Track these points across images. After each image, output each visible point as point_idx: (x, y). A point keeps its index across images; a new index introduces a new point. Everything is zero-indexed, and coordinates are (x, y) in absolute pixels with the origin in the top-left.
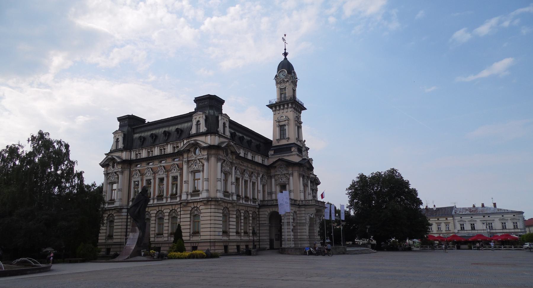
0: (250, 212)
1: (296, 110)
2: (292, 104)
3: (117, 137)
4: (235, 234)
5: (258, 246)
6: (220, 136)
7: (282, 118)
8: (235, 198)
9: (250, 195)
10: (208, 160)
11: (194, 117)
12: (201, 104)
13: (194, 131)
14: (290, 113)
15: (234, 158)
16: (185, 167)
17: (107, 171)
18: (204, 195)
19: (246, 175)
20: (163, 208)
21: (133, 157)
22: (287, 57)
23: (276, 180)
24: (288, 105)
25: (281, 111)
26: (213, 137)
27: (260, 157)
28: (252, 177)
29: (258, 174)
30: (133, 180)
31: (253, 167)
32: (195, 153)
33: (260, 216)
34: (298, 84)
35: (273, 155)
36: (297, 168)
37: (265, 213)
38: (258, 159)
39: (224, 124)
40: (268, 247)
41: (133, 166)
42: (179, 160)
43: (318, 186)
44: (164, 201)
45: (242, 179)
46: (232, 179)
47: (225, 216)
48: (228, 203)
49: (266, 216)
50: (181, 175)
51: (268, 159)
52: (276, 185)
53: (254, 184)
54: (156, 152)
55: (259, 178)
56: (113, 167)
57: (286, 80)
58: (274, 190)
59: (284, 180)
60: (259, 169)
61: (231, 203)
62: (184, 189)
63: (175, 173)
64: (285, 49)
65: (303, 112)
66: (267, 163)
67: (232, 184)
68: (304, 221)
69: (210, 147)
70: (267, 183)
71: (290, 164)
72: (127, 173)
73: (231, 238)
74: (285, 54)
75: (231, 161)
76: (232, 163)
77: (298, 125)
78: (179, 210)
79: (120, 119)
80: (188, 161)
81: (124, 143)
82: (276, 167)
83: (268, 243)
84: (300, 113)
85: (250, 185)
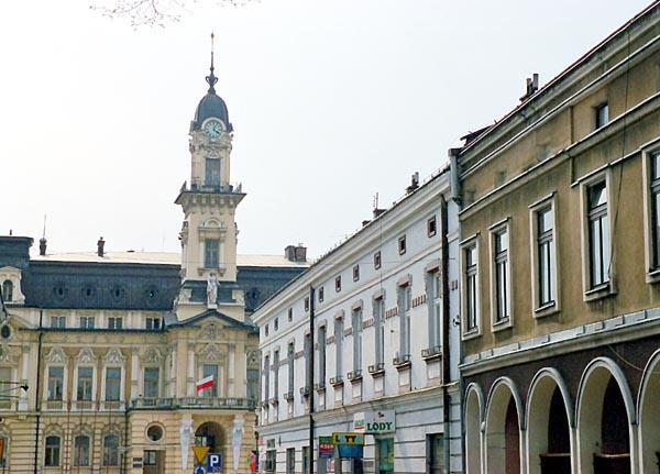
14: (201, 217)
22: (216, 87)
31: (115, 338)
36: (181, 333)
60: (137, 339)
64: (212, 69)
74: (212, 80)
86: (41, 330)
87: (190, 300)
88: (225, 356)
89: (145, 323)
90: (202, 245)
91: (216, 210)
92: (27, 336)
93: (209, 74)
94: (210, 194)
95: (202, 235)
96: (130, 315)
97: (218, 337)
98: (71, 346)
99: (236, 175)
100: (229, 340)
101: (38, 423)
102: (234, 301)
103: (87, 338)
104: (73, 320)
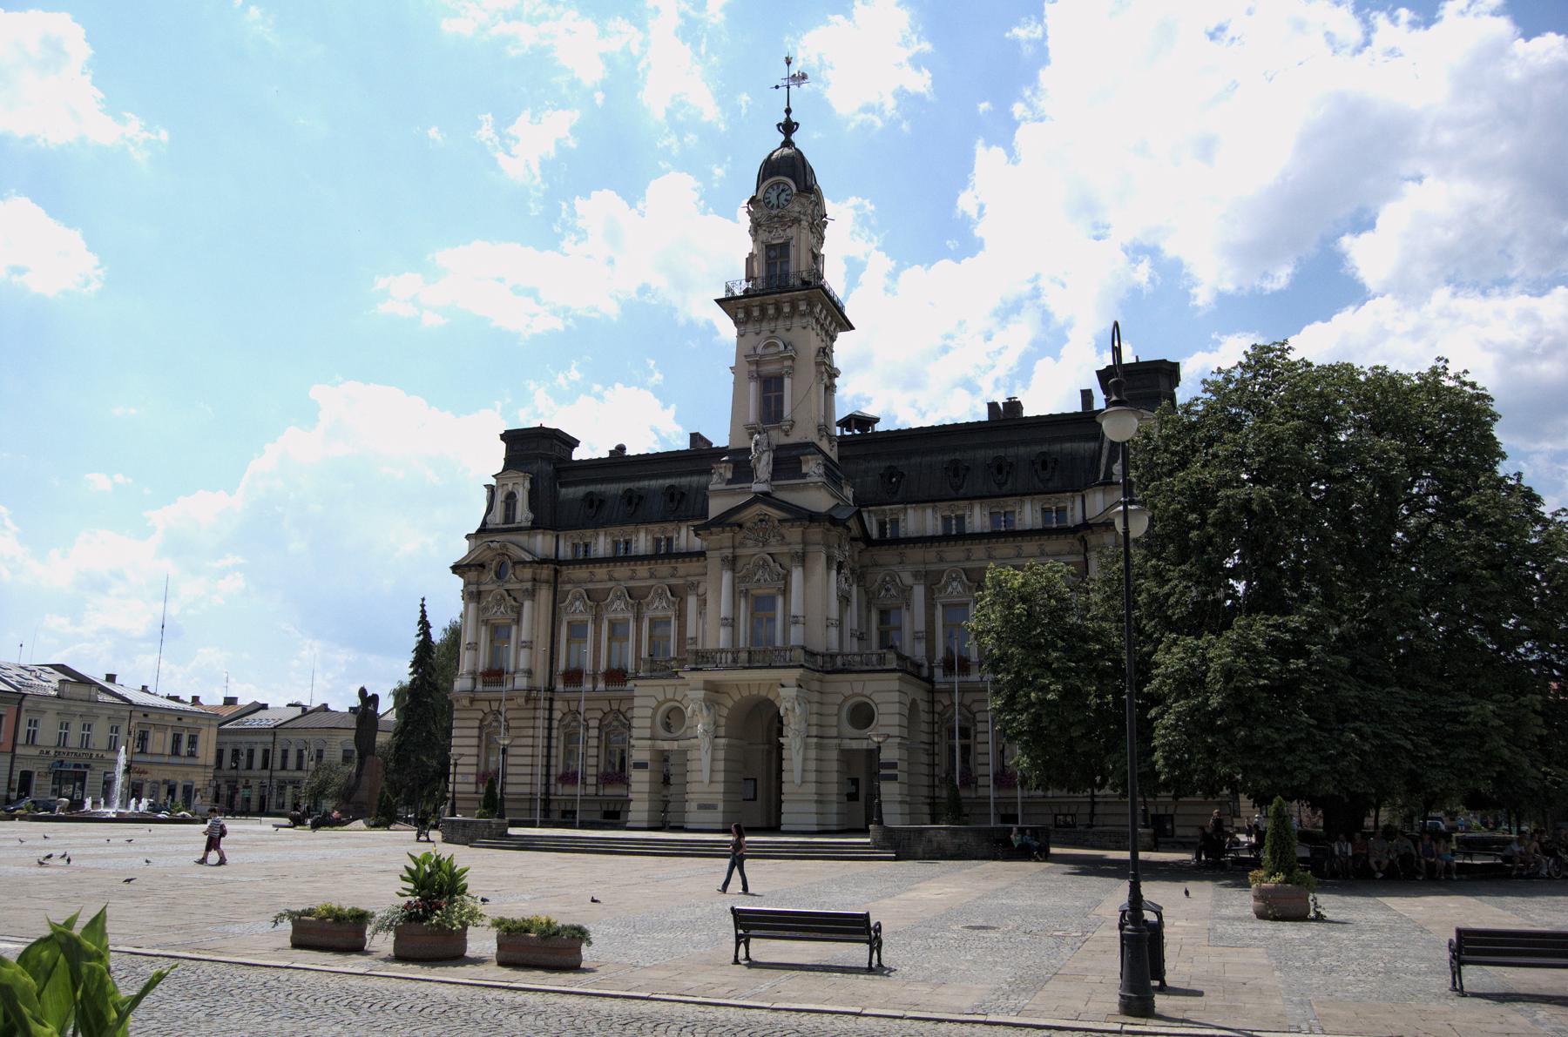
31: (663, 568)
45: (597, 620)
64: (788, 111)
74: (788, 127)
77: (770, 369)
86: (556, 563)
87: (729, 482)
88: (786, 578)
90: (753, 388)
91: (781, 324)
92: (527, 573)
93: (782, 118)
94: (785, 298)
95: (754, 368)
97: (773, 541)
98: (599, 586)
101: (551, 710)
102: (805, 476)
103: (621, 571)
104: (602, 545)
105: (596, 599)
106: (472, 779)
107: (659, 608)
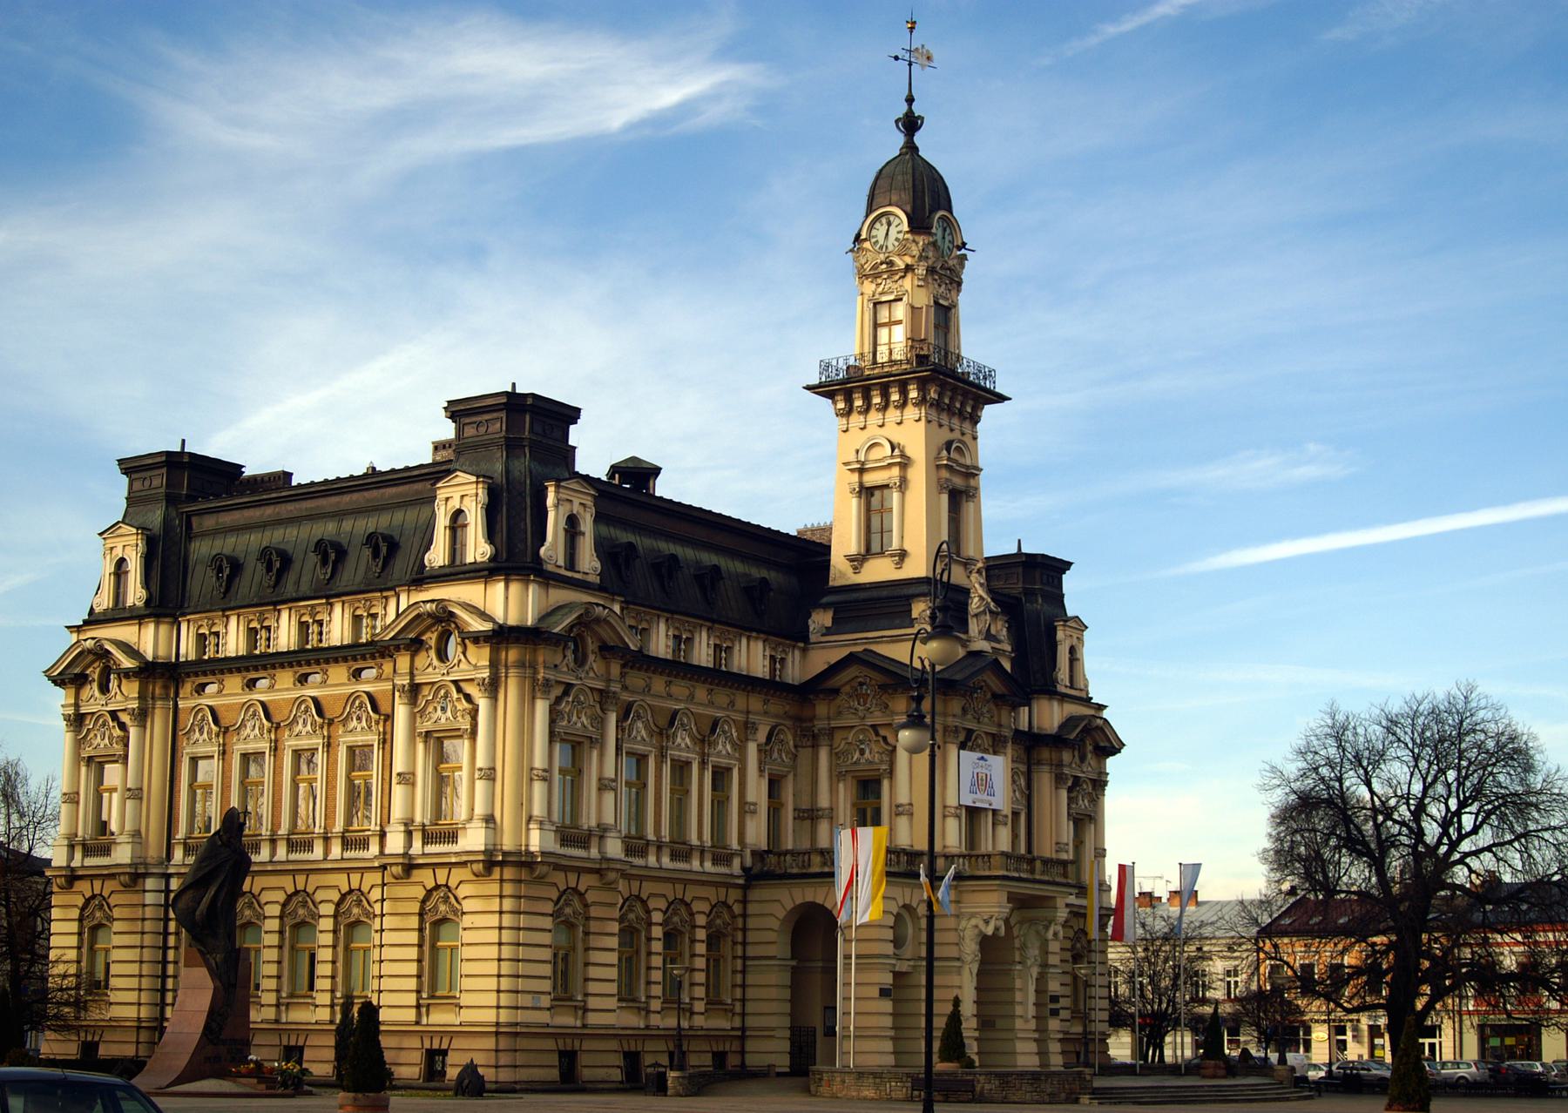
0: (696, 906)
1: (950, 410)
2: (922, 389)
3: (118, 553)
4: (612, 1003)
5: (733, 1061)
6: (547, 578)
7: (876, 454)
8: (614, 848)
9: (698, 831)
10: (493, 687)
11: (441, 494)
12: (470, 431)
13: (437, 556)
15: (615, 669)
16: (401, 713)
17: (77, 705)
18: (474, 839)
19: (683, 739)
20: (315, 880)
21: (188, 649)
22: (919, 139)
23: (835, 755)
24: (904, 393)
25: (874, 417)
26: (515, 588)
27: (760, 645)
28: (713, 744)
29: (748, 728)
30: (187, 751)
31: (722, 697)
32: (442, 656)
33: (751, 923)
34: (966, 276)
35: (828, 631)
37: (774, 907)
38: (751, 657)
39: (572, 521)
40: (783, 1062)
41: (187, 688)
42: (379, 678)
43: (1111, 762)
44: (318, 852)
46: (605, 763)
47: (564, 923)
48: (580, 871)
49: (775, 924)
50: (386, 741)
51: (804, 651)
52: (837, 776)
53: (720, 776)
54: (285, 634)
55: (752, 748)
56: (104, 689)
57: (900, 263)
58: (824, 801)
59: (873, 754)
60: (756, 703)
61: (598, 871)
62: (397, 812)
63: (360, 733)
64: (910, 100)
65: (989, 412)
66: (797, 669)
67: (603, 786)
68: (952, 952)
69: (501, 636)
70: (794, 768)
71: (895, 678)
72: (159, 722)
73: (593, 1019)
74: (911, 124)
75: (600, 685)
76: (604, 696)
77: (958, 482)
78: (376, 894)
79: (130, 467)
80: (414, 690)
81: (147, 582)
82: (836, 692)
83: (786, 1046)
84: (975, 420)
85: (700, 784)
89: (767, 662)
90: (945, 498)
95: (945, 474)
96: (744, 641)
99: (976, 347)
100: (1000, 725)
105: (666, 726)
106: (545, 1001)
107: (722, 749)
